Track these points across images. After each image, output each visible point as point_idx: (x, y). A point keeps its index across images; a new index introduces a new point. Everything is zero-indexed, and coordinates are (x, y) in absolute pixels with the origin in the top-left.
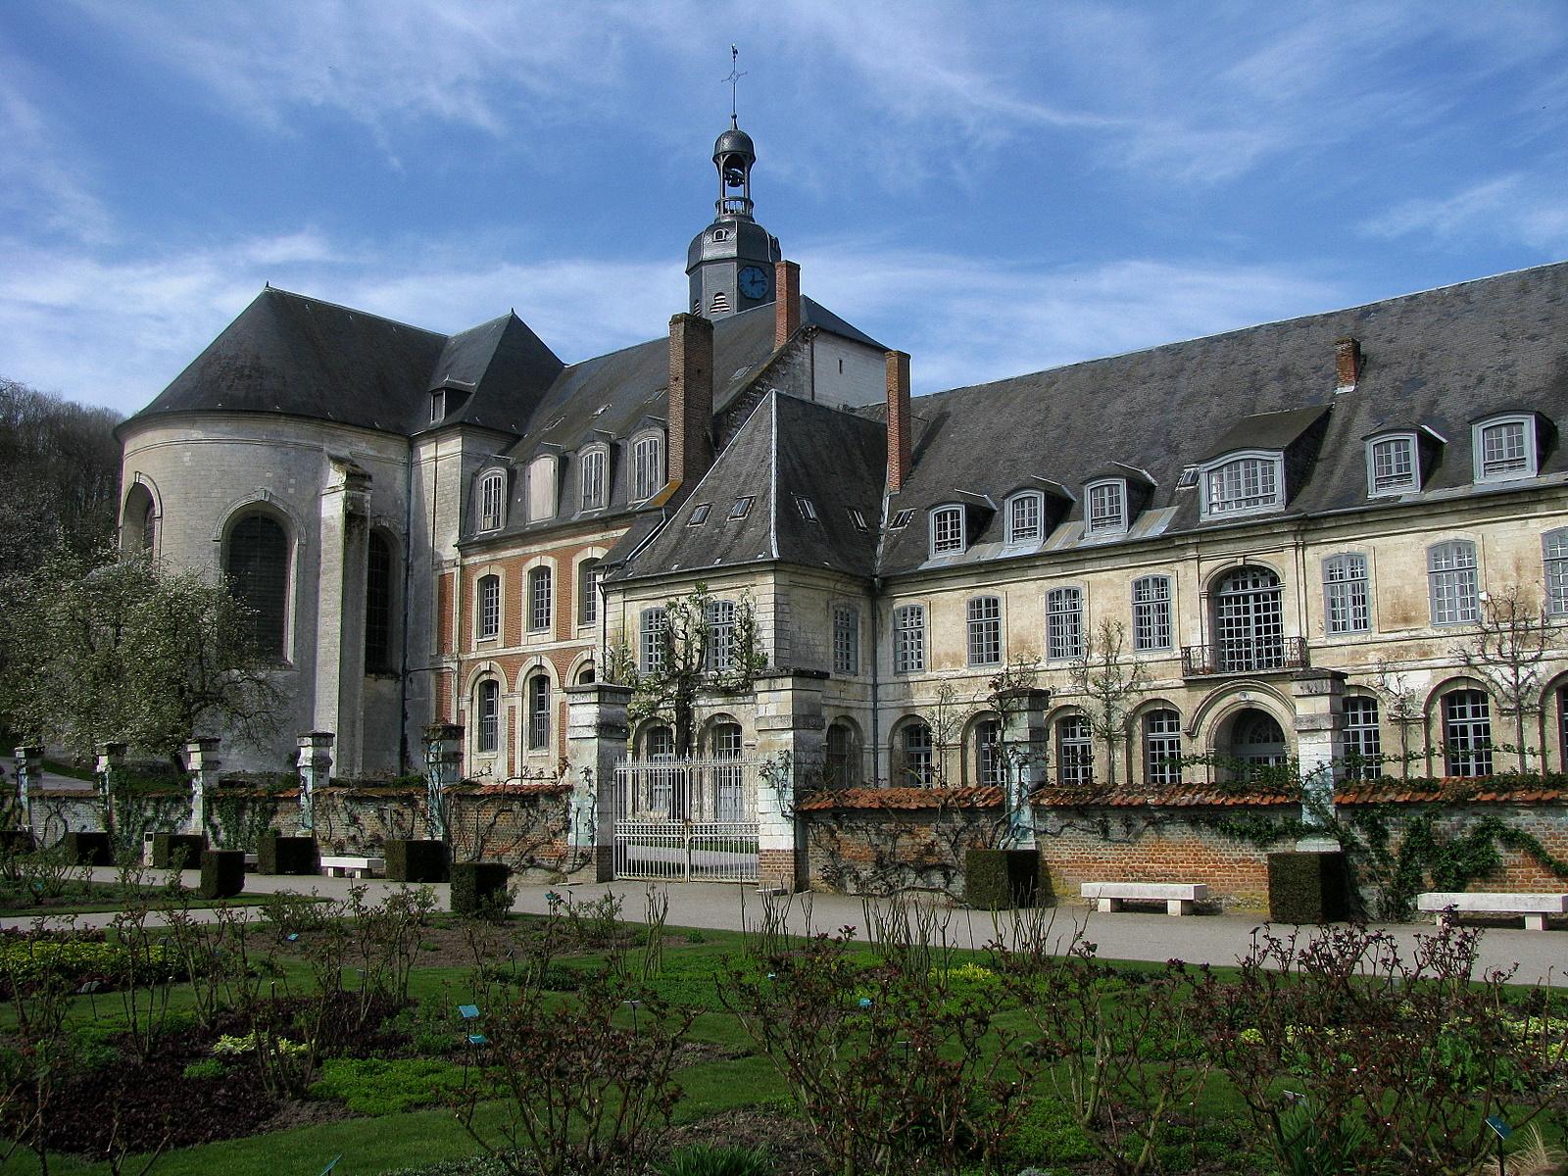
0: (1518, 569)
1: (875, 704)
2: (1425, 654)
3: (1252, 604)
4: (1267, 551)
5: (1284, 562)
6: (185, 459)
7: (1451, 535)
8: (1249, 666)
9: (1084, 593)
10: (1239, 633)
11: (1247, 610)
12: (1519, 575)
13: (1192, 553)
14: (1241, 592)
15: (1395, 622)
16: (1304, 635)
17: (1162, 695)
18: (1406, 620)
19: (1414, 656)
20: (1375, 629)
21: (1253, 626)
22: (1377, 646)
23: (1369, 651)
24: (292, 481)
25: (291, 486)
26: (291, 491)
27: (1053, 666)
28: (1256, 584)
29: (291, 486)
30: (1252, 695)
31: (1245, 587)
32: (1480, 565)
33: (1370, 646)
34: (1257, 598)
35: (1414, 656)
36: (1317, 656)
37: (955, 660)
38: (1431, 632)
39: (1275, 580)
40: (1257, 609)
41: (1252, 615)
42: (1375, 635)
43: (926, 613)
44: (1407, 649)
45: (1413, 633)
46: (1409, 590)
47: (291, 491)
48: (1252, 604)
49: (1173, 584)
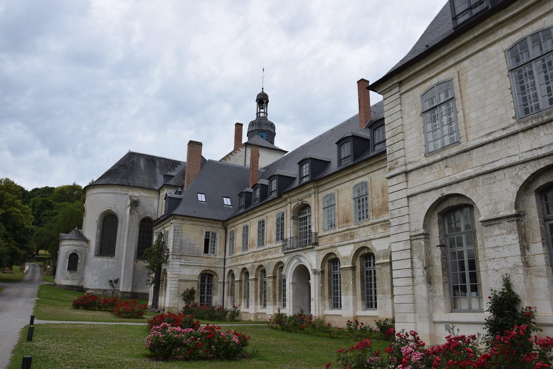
0: (383, 192)
1: (224, 266)
5: (311, 201)
12: (383, 194)
15: (343, 223)
16: (317, 231)
19: (349, 238)
20: (337, 227)
22: (338, 234)
23: (335, 237)
24: (119, 204)
25: (118, 205)
26: (118, 206)
29: (118, 205)
32: (369, 192)
33: (336, 235)
35: (349, 238)
36: (321, 240)
42: (337, 230)
44: (347, 235)
45: (348, 227)
47: (118, 206)
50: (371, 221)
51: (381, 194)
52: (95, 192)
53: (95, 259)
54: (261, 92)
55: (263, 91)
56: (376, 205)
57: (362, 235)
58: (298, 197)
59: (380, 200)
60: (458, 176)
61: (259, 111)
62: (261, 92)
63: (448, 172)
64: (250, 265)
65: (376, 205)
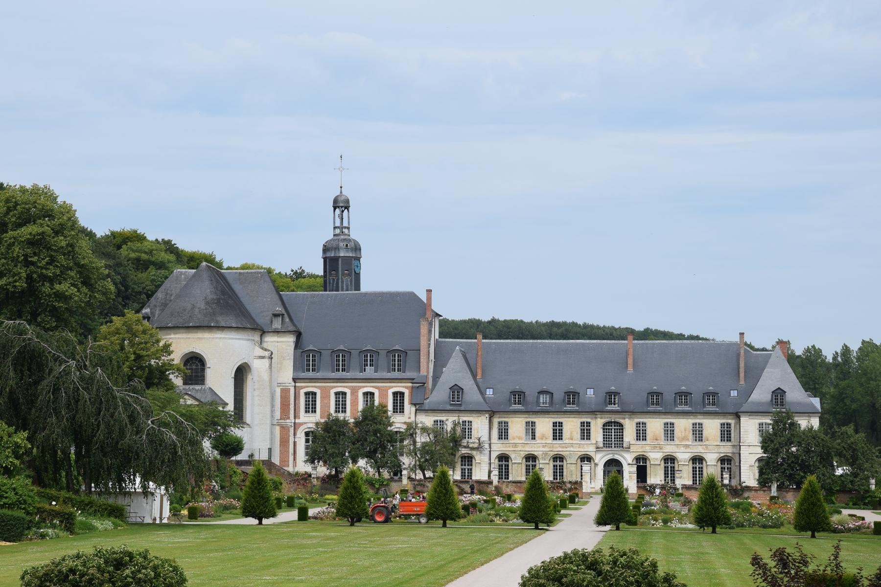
2: (661, 449)
3: (613, 431)
4: (620, 418)
7: (669, 421)
11: (611, 432)
13: (599, 416)
14: (610, 427)
17: (587, 453)
18: (656, 440)
21: (613, 437)
30: (616, 456)
31: (611, 426)
34: (615, 429)
37: (520, 438)
39: (622, 426)
40: (615, 432)
41: (613, 434)
43: (510, 424)
44: (656, 447)
48: (613, 431)
49: (592, 425)
50: (676, 443)
51: (683, 430)
55: (341, 192)
56: (680, 436)
57: (670, 449)
59: (683, 434)
61: (338, 224)
62: (339, 193)
65: (680, 436)
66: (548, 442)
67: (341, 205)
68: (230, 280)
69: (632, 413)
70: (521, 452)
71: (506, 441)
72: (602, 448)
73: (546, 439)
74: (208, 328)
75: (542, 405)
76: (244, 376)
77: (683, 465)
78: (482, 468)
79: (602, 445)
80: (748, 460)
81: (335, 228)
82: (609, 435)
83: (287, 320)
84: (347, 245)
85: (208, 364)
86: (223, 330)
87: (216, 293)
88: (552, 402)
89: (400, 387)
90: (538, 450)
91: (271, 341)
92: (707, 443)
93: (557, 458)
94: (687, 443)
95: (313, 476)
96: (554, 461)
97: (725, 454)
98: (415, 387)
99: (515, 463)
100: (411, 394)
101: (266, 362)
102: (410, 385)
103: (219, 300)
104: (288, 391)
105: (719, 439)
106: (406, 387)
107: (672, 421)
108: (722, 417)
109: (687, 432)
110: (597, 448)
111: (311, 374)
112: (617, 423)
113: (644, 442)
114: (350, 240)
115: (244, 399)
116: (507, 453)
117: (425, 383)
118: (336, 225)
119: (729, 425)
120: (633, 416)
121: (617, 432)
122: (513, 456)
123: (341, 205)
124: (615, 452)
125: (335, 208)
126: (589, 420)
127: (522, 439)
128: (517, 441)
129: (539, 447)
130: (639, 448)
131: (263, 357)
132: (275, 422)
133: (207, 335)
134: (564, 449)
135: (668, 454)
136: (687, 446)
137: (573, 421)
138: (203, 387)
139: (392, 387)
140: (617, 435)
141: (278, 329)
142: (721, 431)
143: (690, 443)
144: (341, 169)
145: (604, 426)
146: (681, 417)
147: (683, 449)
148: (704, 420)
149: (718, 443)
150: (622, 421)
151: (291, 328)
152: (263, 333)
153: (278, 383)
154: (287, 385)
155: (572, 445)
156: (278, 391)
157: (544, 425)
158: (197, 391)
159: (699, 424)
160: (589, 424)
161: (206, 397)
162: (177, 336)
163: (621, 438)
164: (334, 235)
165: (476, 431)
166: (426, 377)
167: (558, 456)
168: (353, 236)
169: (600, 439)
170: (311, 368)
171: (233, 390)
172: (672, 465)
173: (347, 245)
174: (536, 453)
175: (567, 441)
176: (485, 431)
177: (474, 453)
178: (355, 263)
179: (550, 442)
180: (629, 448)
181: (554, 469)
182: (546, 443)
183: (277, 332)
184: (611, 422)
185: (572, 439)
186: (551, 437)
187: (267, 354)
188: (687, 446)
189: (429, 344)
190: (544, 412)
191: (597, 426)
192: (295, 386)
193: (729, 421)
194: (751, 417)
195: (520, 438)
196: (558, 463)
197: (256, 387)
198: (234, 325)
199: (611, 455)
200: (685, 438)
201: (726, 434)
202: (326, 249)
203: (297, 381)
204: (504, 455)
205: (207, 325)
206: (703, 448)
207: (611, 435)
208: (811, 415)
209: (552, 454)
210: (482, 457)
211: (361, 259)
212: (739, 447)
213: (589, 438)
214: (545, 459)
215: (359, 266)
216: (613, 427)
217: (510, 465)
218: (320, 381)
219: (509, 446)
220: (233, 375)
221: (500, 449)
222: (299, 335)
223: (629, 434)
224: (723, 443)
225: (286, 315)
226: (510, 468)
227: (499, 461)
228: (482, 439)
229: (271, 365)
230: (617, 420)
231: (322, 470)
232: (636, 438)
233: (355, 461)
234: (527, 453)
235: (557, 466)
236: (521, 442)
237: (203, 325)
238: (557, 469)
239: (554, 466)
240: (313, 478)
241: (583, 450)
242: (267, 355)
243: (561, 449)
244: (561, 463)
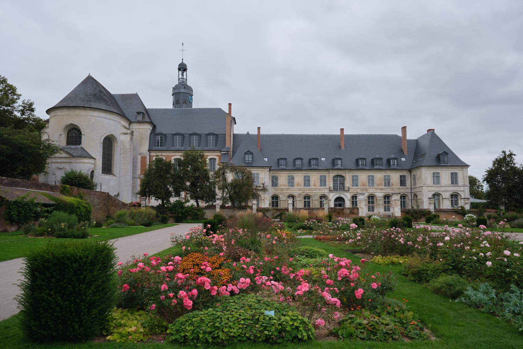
0: (380, 180)
3: (338, 181)
4: (343, 173)
6: (92, 120)
7: (371, 174)
8: (338, 190)
9: (311, 176)
10: (336, 185)
11: (338, 182)
13: (331, 172)
17: (324, 194)
18: (364, 185)
27: (305, 188)
28: (339, 178)
34: (339, 180)
35: (365, 190)
37: (285, 185)
38: (367, 187)
39: (344, 177)
40: (339, 182)
44: (364, 190)
46: (364, 181)
48: (338, 181)
50: (375, 187)
51: (379, 180)
52: (95, 115)
53: (103, 177)
54: (181, 62)
55: (182, 62)
57: (371, 191)
58: (337, 172)
59: (379, 182)
60: (440, 190)
63: (437, 189)
64: (297, 194)
66: (301, 188)
67: (183, 68)
68: (116, 99)
69: (351, 170)
70: (286, 194)
71: (276, 188)
72: (333, 191)
73: (300, 186)
74: (84, 108)
75: (297, 166)
76: (113, 145)
77: (379, 200)
78: (265, 202)
79: (332, 189)
80: (428, 195)
81: (179, 79)
82: (336, 183)
83: (146, 117)
84: (185, 87)
85: (82, 133)
86: (95, 111)
87: (94, 91)
88: (302, 165)
89: (213, 155)
90: (295, 192)
91: (135, 127)
92: (393, 187)
93: (306, 197)
94: (382, 187)
95: (142, 205)
96: (304, 199)
97: (403, 193)
98: (222, 154)
99: (282, 200)
100: (220, 159)
101: (128, 137)
102: (219, 154)
103: (95, 95)
104: (145, 158)
105: (399, 184)
106: (217, 156)
107: (373, 174)
108: (400, 172)
109: (381, 181)
110: (330, 191)
111: (160, 148)
112: (341, 176)
113: (357, 187)
114: (187, 85)
115: (113, 159)
116: (277, 194)
117: (229, 152)
118: (180, 78)
119: (404, 176)
120: (350, 172)
121: (341, 182)
122: (281, 196)
123: (183, 68)
124: (341, 193)
125: (179, 69)
126: (325, 174)
127: (286, 186)
128: (283, 187)
129: (296, 190)
130: (354, 190)
131: (126, 134)
132: (137, 176)
133: (82, 112)
134: (311, 192)
135: (371, 193)
136: (381, 189)
137: (315, 175)
138: (77, 147)
139: (209, 156)
140: (341, 183)
141: (140, 121)
142: (401, 180)
143: (383, 187)
144: (183, 50)
145: (333, 178)
146: (377, 172)
147: (379, 191)
148: (391, 174)
149: (399, 187)
150: (344, 175)
151: (148, 120)
152: (131, 123)
153: (139, 153)
154: (145, 154)
155: (315, 189)
156: (139, 158)
157: (299, 177)
158: (72, 149)
159: (389, 176)
160: (325, 177)
161: (77, 153)
162: (62, 114)
163: (343, 184)
164: (179, 83)
165: (261, 180)
166: (230, 148)
167: (307, 196)
168: (188, 84)
169: (332, 185)
170: (160, 144)
171: (101, 151)
172: (372, 200)
173: (185, 87)
174: (294, 194)
175: (312, 187)
176: (267, 179)
177: (260, 193)
178: (190, 97)
179: (303, 187)
180: (349, 190)
181: (304, 204)
182: (300, 188)
183: (139, 122)
184: (337, 176)
185: (315, 186)
186: (303, 185)
187: (129, 131)
188: (381, 189)
189: (231, 131)
190: (300, 170)
191: (330, 176)
192: (150, 155)
193: (405, 174)
194: (428, 169)
195: (285, 185)
196: (307, 200)
197: (122, 152)
198: (103, 108)
199: (339, 195)
200: (380, 184)
201: (403, 182)
202: (174, 89)
203: (151, 152)
204: (275, 196)
205: (82, 105)
206: (390, 190)
207: (338, 183)
208: (463, 167)
209: (304, 194)
210: (265, 196)
211: (193, 97)
212: (410, 189)
213: (325, 185)
214: (299, 198)
215: (192, 99)
216: (338, 179)
217: (279, 202)
218: (165, 152)
219: (279, 191)
220: (102, 141)
221: (274, 192)
222: (154, 127)
223: (348, 183)
224: (402, 187)
225: (146, 114)
226: (279, 203)
227: (272, 199)
228: (265, 185)
229: (131, 139)
230: (342, 174)
231: (154, 202)
232: (352, 185)
233: (178, 194)
234: (289, 194)
235: (306, 201)
236: (285, 187)
237: (78, 106)
238: (306, 203)
239: (304, 202)
240: (143, 207)
241: (322, 192)
242: (129, 132)
243: (309, 192)
244: (308, 200)
